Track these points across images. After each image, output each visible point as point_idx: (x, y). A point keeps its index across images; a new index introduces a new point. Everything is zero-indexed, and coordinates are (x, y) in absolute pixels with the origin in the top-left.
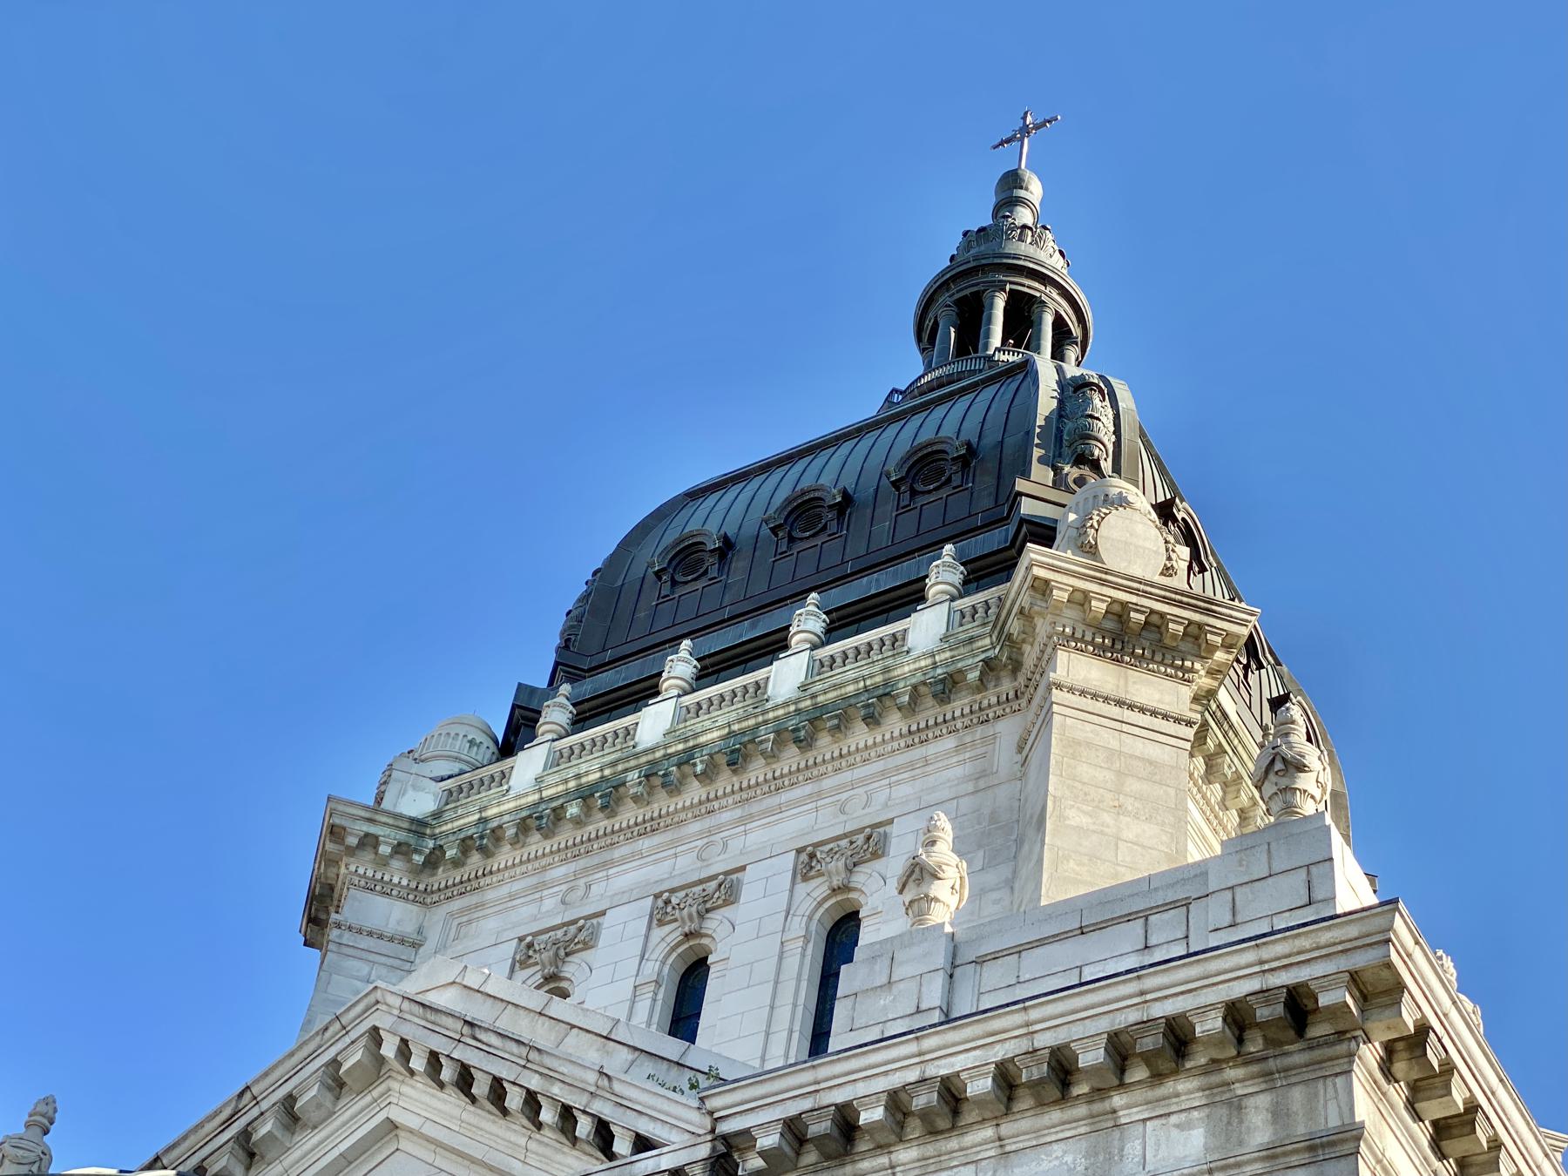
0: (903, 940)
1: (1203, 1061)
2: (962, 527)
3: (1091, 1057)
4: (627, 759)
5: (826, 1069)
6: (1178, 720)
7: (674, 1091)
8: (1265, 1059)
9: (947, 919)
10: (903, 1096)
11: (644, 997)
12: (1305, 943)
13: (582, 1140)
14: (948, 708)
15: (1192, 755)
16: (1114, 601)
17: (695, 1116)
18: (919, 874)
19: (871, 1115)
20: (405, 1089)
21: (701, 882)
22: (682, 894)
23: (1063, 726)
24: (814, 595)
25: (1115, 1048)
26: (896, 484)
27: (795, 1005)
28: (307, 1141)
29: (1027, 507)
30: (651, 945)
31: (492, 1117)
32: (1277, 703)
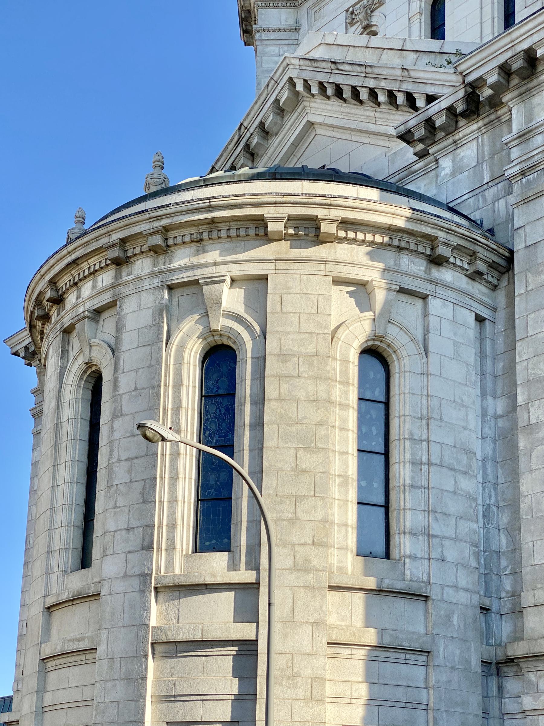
7: (441, 67)
11: (414, 23)
13: (401, 105)
31: (356, 106)
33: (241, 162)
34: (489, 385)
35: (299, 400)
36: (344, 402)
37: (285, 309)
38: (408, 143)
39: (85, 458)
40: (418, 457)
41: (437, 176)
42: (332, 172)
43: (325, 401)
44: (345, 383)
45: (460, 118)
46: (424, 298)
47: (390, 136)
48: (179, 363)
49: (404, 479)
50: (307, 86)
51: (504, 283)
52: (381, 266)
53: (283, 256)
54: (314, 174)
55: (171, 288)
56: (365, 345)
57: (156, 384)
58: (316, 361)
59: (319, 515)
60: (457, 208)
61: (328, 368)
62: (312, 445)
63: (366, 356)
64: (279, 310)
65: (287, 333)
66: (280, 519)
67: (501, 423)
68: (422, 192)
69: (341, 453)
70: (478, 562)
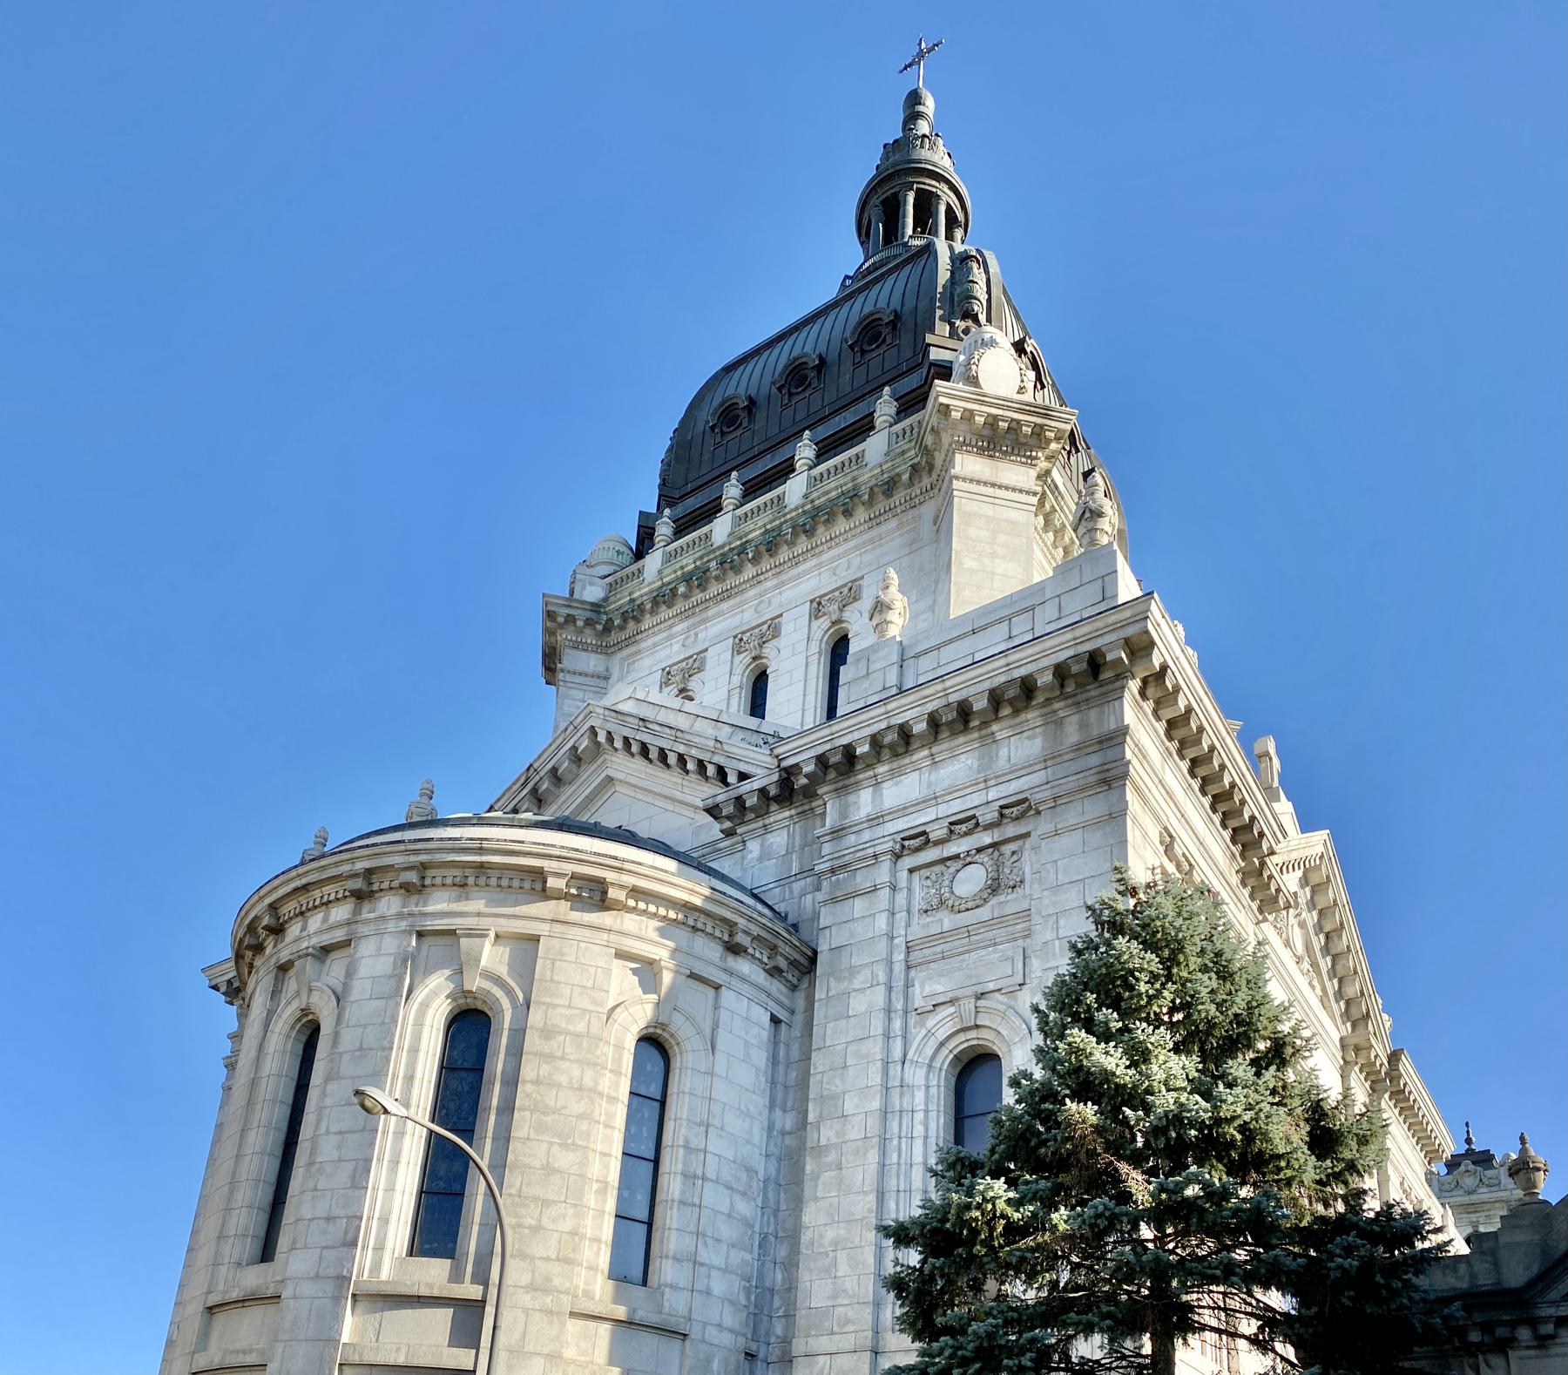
0: (873, 649)
2: (894, 373)
4: (708, 554)
5: (836, 726)
6: (1028, 493)
8: (1075, 695)
9: (897, 633)
10: (878, 737)
12: (1100, 624)
15: (1036, 515)
17: (769, 759)
18: (880, 607)
19: (862, 749)
20: (613, 759)
21: (758, 626)
22: (749, 634)
23: (960, 503)
24: (807, 432)
25: (993, 698)
26: (851, 347)
27: (817, 693)
29: (935, 354)
30: (735, 664)
33: (526, 806)
34: (780, 1096)
35: (559, 1086)
36: (613, 1094)
37: (556, 978)
38: (716, 818)
39: (284, 1126)
40: (692, 1170)
41: (743, 858)
42: (627, 834)
43: (590, 1090)
44: (617, 1072)
45: (772, 803)
46: (717, 987)
47: (697, 808)
48: (419, 1024)
49: (673, 1192)
50: (610, 738)
51: (805, 985)
53: (561, 917)
54: (606, 833)
55: (420, 935)
56: (645, 1032)
57: (387, 1045)
58: (585, 1044)
59: (567, 1225)
60: (762, 896)
61: (599, 1052)
62: (569, 1141)
63: (644, 1045)
65: (555, 1006)
67: (788, 1140)
68: (725, 872)
69: (603, 1154)
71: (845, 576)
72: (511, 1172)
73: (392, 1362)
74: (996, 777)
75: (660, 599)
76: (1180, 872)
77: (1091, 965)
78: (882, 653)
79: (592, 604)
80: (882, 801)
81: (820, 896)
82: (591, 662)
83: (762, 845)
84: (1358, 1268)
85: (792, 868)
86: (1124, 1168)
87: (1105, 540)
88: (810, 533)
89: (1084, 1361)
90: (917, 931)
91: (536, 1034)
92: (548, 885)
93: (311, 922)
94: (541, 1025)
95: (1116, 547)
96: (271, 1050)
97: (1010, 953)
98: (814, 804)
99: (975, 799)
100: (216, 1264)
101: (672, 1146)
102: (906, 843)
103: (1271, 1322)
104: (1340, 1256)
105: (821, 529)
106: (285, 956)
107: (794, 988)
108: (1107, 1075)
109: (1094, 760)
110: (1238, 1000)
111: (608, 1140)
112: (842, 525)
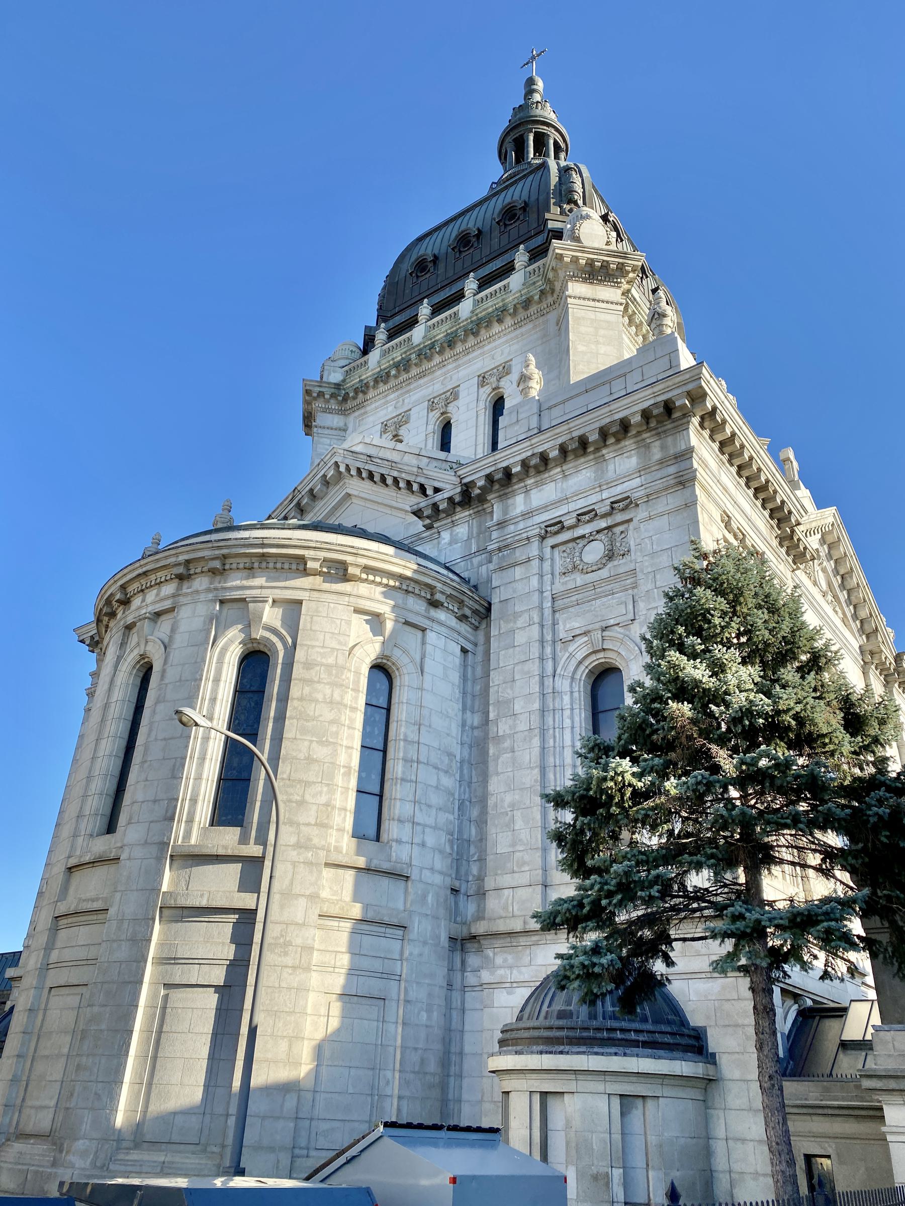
1: (634, 432)
3: (593, 437)
5: (498, 455)
8: (657, 428)
14: (528, 312)
16: (588, 259)
17: (454, 478)
18: (524, 379)
19: (516, 469)
28: (320, 504)
32: (654, 291)
34: (469, 702)
35: (317, 701)
36: (354, 705)
37: (313, 628)
38: (419, 517)
39: (126, 736)
40: (409, 756)
41: (439, 543)
43: (338, 703)
44: (356, 690)
46: (424, 630)
48: (220, 661)
51: (484, 626)
52: (392, 603)
59: (323, 799)
61: (344, 677)
63: (375, 671)
64: (309, 628)
65: (313, 647)
66: (290, 801)
69: (348, 747)
70: (452, 848)
71: (500, 359)
72: (283, 762)
73: (197, 904)
74: (607, 484)
75: (379, 379)
76: (736, 539)
77: (680, 607)
78: (526, 408)
79: (335, 384)
80: (531, 502)
81: (492, 566)
82: (336, 420)
83: (451, 534)
84: (889, 814)
85: (471, 549)
86: (714, 748)
87: (669, 331)
88: (476, 334)
89: (697, 890)
90: (559, 587)
91: (301, 666)
92: (308, 566)
93: (147, 596)
94: (303, 660)
95: (676, 335)
96: (119, 683)
97: (623, 599)
98: (485, 506)
99: (593, 499)
100: (75, 836)
101: (396, 740)
102: (549, 529)
103: (829, 854)
104: (875, 806)
105: (483, 331)
106: (130, 619)
107: (476, 628)
108: (697, 683)
109: (672, 470)
110: (784, 627)
111: (351, 737)
112: (496, 328)
